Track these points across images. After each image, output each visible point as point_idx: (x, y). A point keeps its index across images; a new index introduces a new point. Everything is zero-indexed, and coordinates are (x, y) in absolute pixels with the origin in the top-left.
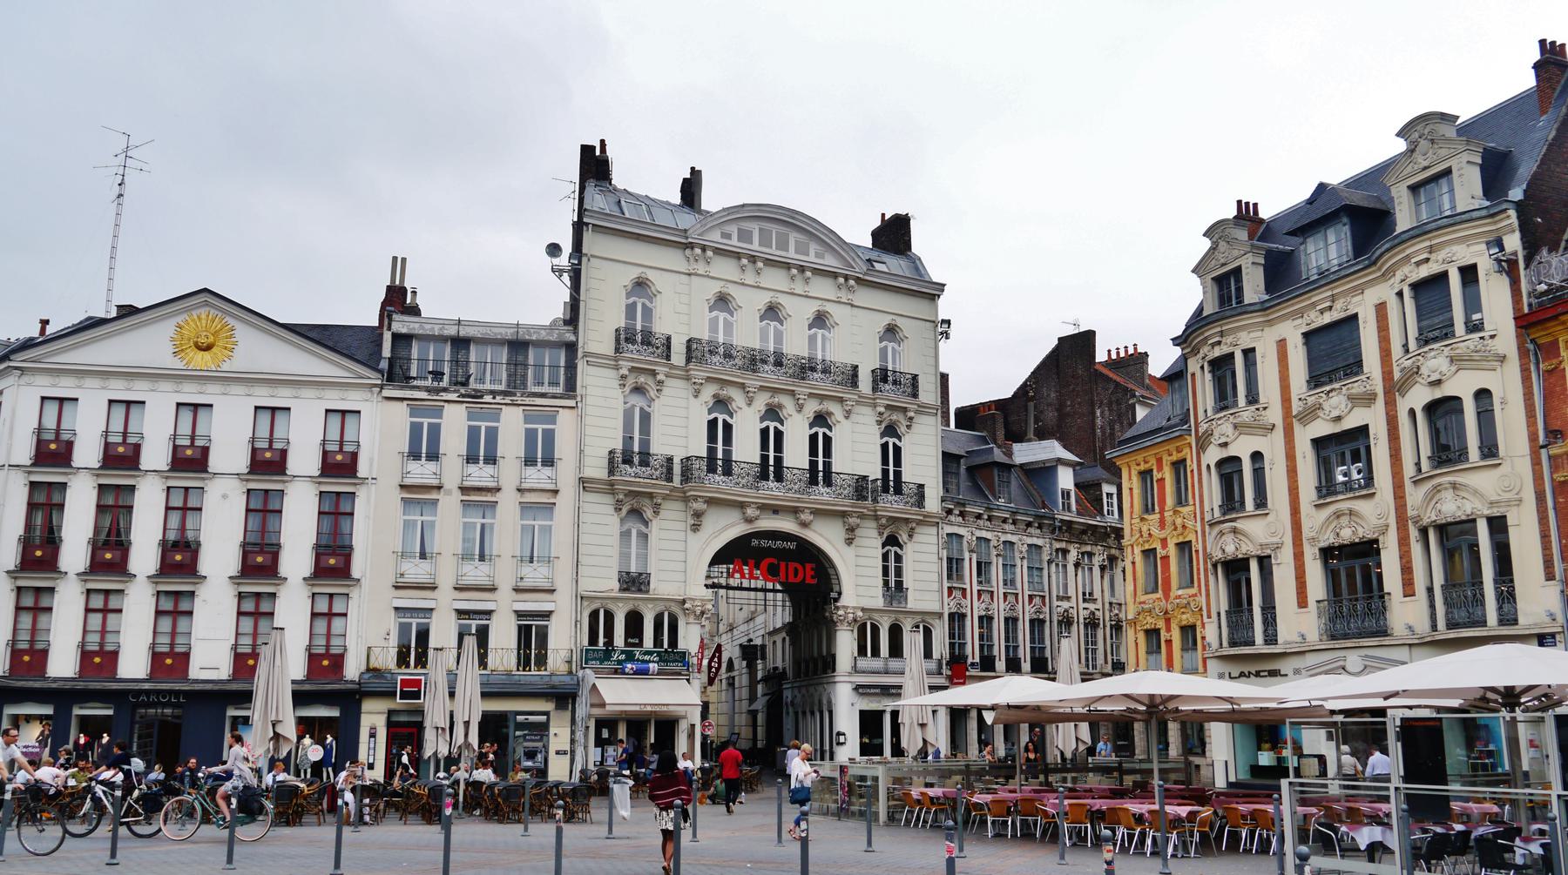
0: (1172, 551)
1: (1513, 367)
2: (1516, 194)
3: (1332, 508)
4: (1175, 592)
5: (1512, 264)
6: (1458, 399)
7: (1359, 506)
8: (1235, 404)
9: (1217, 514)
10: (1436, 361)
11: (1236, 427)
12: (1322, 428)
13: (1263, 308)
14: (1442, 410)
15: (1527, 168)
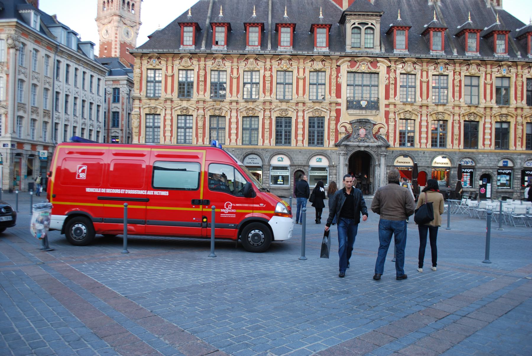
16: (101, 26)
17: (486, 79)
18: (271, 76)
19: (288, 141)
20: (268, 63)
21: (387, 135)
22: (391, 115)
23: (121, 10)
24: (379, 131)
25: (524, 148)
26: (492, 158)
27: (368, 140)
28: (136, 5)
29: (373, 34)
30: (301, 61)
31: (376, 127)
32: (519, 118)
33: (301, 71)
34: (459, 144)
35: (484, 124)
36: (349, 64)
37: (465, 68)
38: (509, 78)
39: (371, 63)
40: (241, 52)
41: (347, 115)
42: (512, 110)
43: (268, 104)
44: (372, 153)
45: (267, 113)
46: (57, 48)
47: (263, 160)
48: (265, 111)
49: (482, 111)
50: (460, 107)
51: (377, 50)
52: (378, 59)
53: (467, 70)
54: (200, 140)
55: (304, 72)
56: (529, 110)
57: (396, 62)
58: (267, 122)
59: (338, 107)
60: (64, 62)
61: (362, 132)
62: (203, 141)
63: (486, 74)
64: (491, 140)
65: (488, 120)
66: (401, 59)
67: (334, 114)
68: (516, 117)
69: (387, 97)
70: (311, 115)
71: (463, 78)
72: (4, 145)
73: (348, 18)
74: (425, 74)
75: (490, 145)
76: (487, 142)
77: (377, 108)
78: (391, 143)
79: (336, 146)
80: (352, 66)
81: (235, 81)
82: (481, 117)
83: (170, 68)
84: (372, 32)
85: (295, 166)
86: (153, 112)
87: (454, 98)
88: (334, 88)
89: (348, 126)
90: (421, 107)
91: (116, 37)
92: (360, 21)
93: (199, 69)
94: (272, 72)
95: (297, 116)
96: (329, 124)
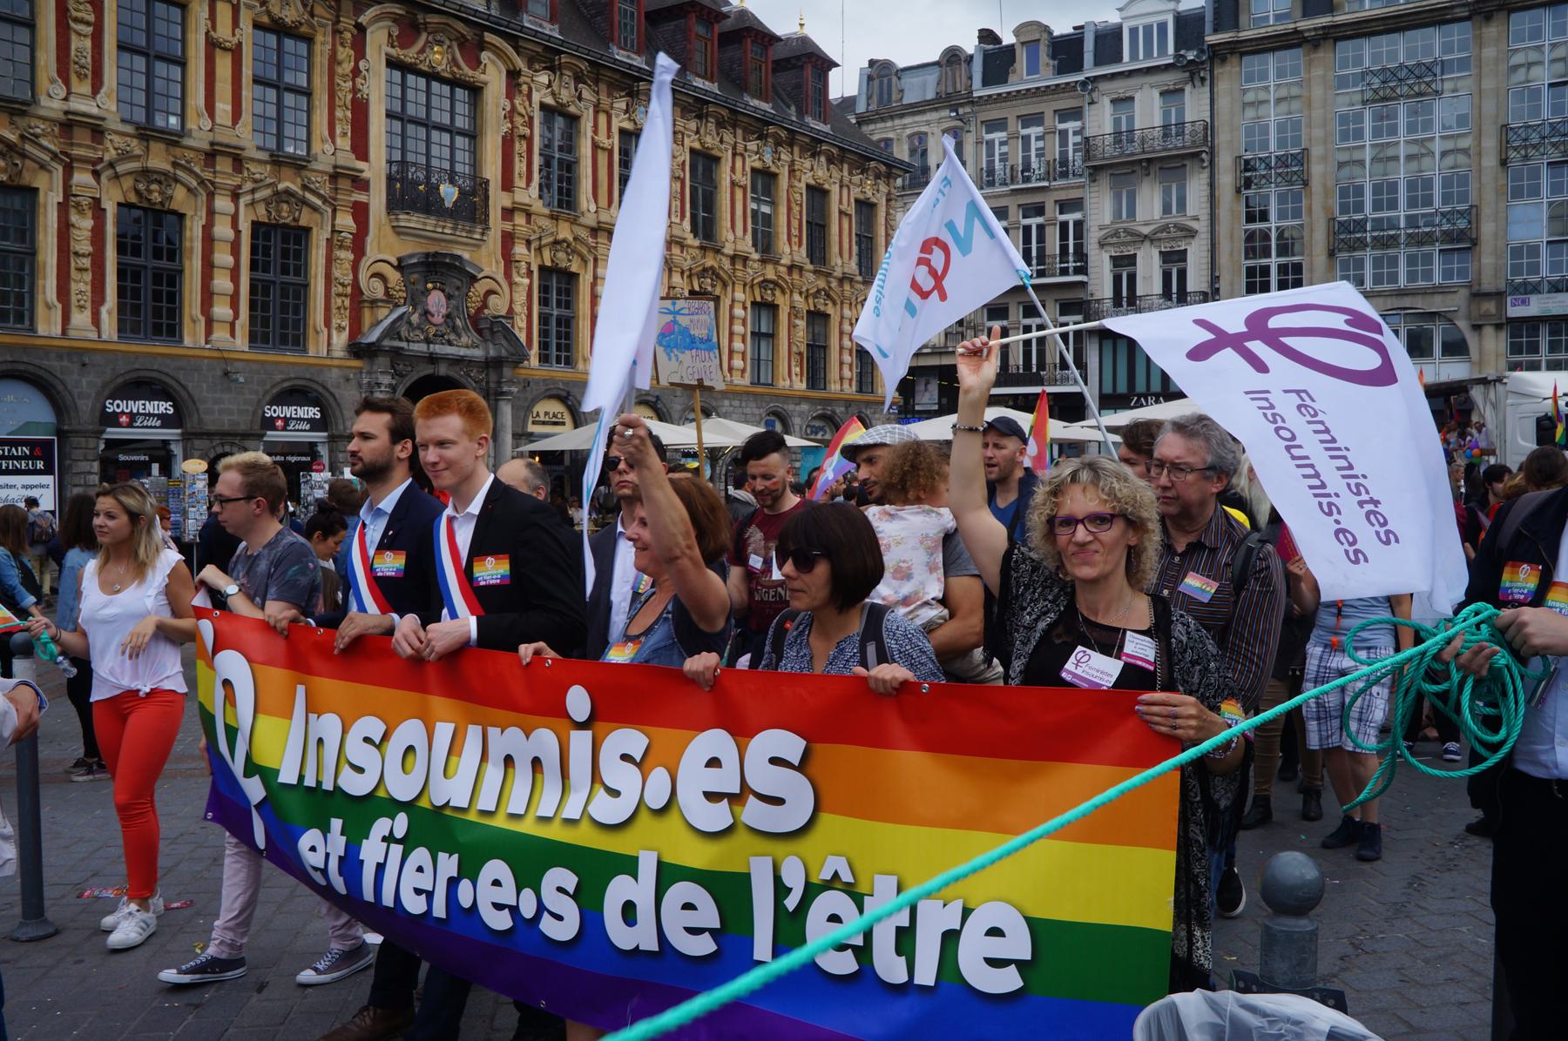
17: (733, 169)
19: (167, 324)
24: (485, 305)
26: (748, 411)
27: (452, 337)
35: (731, 307)
39: (463, 43)
41: (388, 230)
43: (81, 136)
47: (59, 406)
48: (68, 171)
52: (489, 37)
59: (361, 197)
67: (346, 221)
69: (508, 185)
70: (261, 213)
80: (405, 40)
85: (209, 435)
89: (394, 276)
95: (211, 213)
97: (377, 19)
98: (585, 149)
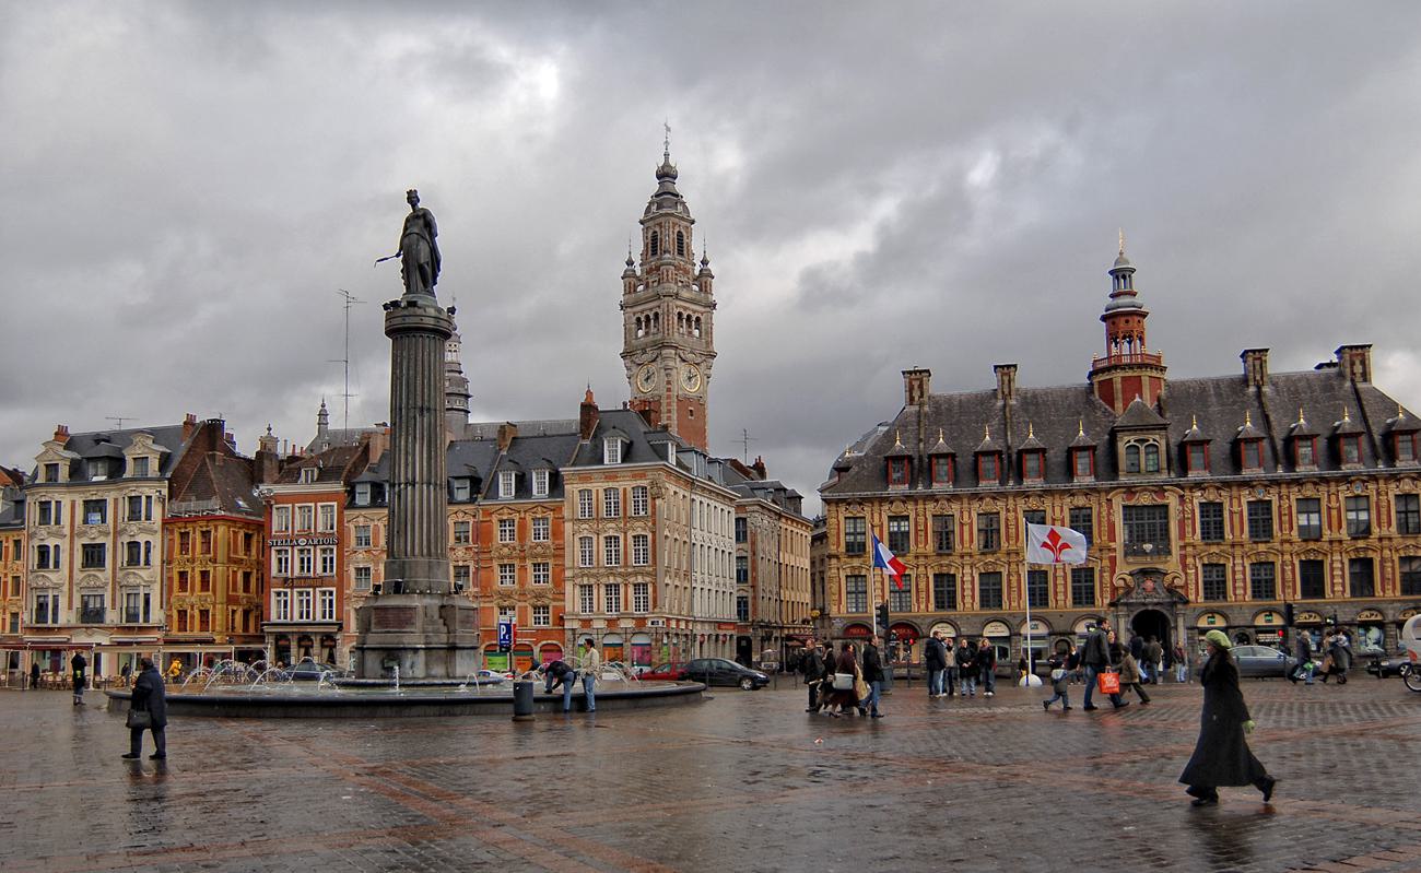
0: (10, 580)
1: (159, 535)
2: (169, 475)
3: (86, 574)
4: (9, 597)
5: (164, 499)
6: (139, 543)
7: (99, 574)
8: (49, 524)
9: (35, 567)
10: (134, 527)
11: (48, 533)
12: (87, 541)
13: (67, 485)
14: (133, 545)
15: (174, 464)
16: (635, 369)
18: (1017, 518)
20: (1011, 501)
21: (1185, 587)
22: (1190, 560)
23: (676, 334)
25: (1398, 593)
28: (702, 318)
29: (1157, 452)
30: (1057, 496)
31: (1169, 577)
32: (1387, 553)
33: (1057, 510)
34: (1295, 592)
35: (1332, 564)
36: (1125, 496)
37: (1296, 489)
38: (1368, 497)
40: (972, 490)
42: (1373, 540)
44: (1165, 612)
45: (1013, 566)
46: (693, 483)
49: (1326, 546)
50: (1291, 542)
51: (1164, 476)
52: (1166, 487)
53: (1299, 491)
54: (923, 606)
55: (1062, 511)
56: (1401, 540)
57: (1191, 489)
58: (1014, 579)
60: (698, 499)
61: (1149, 584)
62: (927, 606)
63: (1329, 495)
64: (1343, 585)
65: (1337, 557)
66: (1199, 486)
67: (1106, 563)
68: (1382, 551)
69: (1182, 536)
71: (1294, 504)
72: (653, 623)
73: (1119, 435)
74: (1235, 502)
75: (1344, 591)
76: (1338, 588)
77: (1169, 553)
78: (1192, 597)
79: (1112, 604)
81: (966, 528)
82: (1325, 555)
83: (876, 516)
84: (1155, 450)
86: (856, 573)
87: (1281, 531)
88: (1105, 528)
89: (1128, 578)
90: (1233, 546)
91: (669, 390)
92: (1137, 437)
93: (917, 515)
94: (1016, 513)
96: (1101, 577)
97: (1114, 496)
98: (1226, 514)
